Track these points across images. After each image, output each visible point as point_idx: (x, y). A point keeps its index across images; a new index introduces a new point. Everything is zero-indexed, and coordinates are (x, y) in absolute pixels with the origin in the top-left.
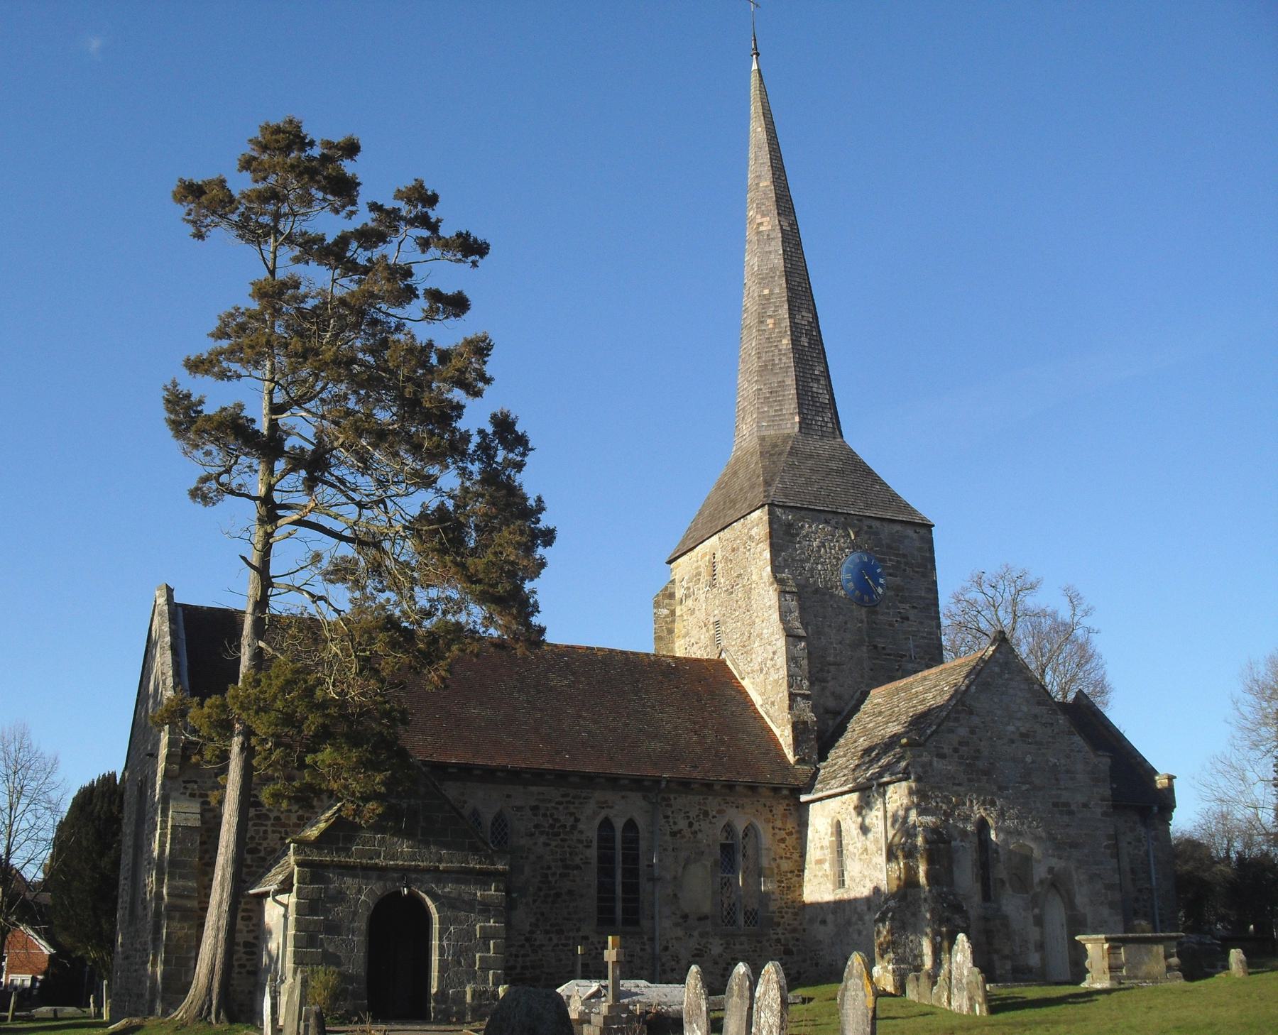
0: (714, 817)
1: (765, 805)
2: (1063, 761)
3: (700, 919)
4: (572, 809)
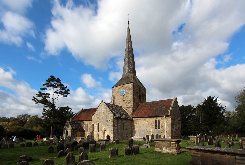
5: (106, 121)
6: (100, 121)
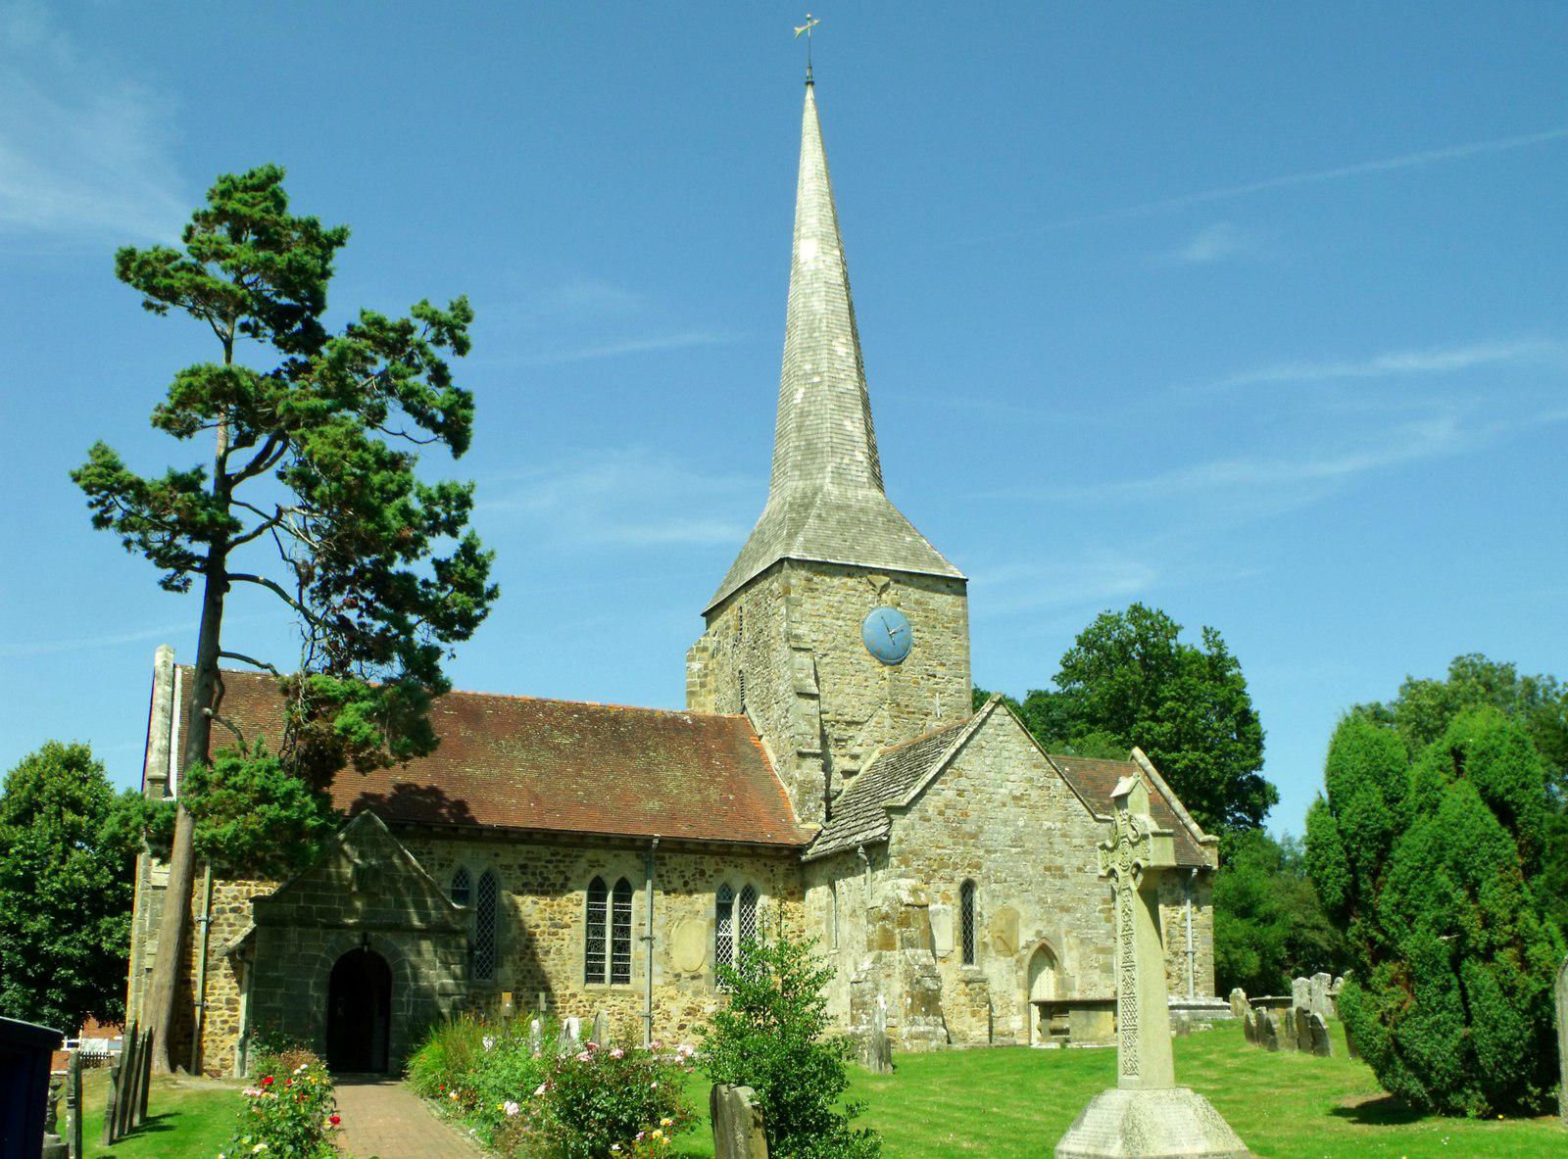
0: (711, 876)
1: (765, 865)
2: (1059, 825)
3: (693, 978)
4: (562, 868)
5: (1048, 869)
6: (986, 865)
